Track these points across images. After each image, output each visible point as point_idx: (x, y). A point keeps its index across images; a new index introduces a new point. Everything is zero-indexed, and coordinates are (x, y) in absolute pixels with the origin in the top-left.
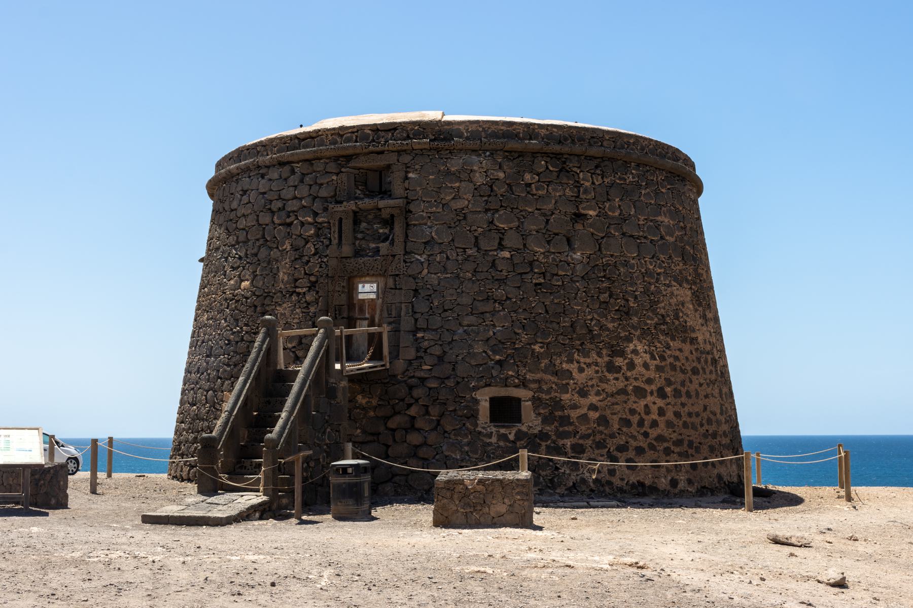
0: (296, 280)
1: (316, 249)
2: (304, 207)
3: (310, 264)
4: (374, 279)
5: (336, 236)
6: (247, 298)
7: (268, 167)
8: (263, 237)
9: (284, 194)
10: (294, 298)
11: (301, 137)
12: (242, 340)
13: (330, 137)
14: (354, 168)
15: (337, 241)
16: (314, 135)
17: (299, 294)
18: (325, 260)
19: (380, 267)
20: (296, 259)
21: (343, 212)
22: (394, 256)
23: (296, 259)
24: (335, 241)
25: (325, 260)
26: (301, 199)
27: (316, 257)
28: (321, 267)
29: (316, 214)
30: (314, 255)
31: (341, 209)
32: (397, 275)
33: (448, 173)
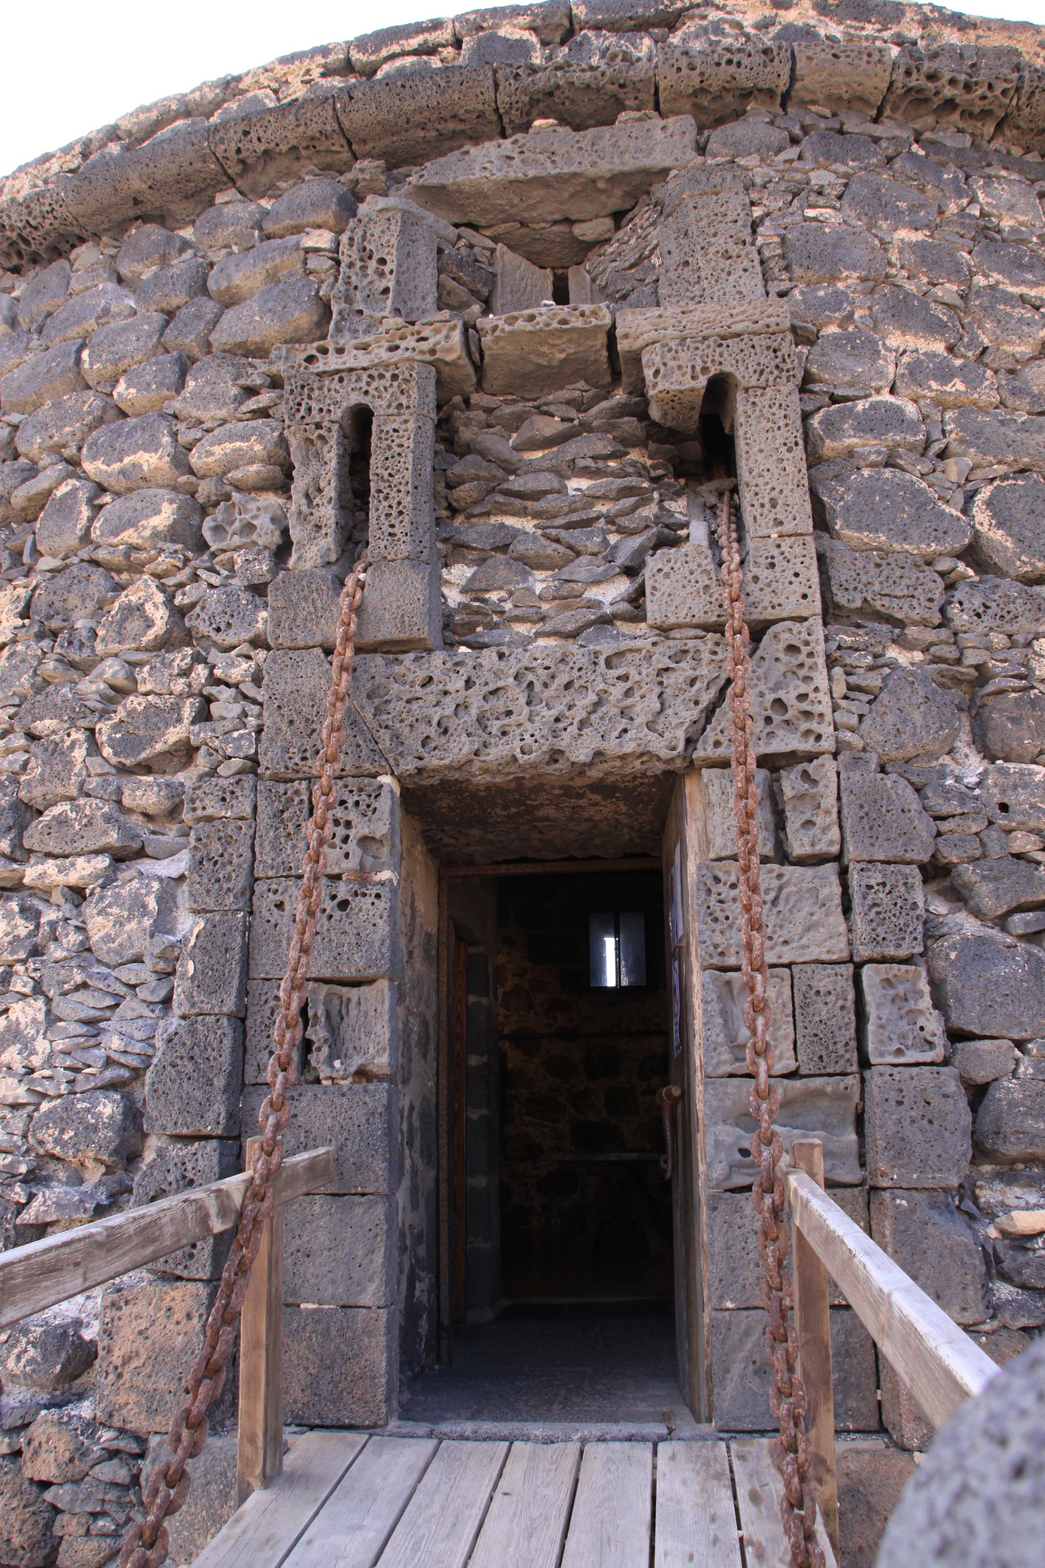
1: (179, 613)
3: (134, 702)
5: (328, 513)
14: (435, 196)
15: (327, 543)
19: (645, 706)
21: (373, 373)
22: (758, 631)
24: (313, 551)
25: (240, 670)
27: (180, 658)
28: (204, 715)
30: (164, 644)
31: (363, 360)
32: (792, 758)
33: (985, 233)
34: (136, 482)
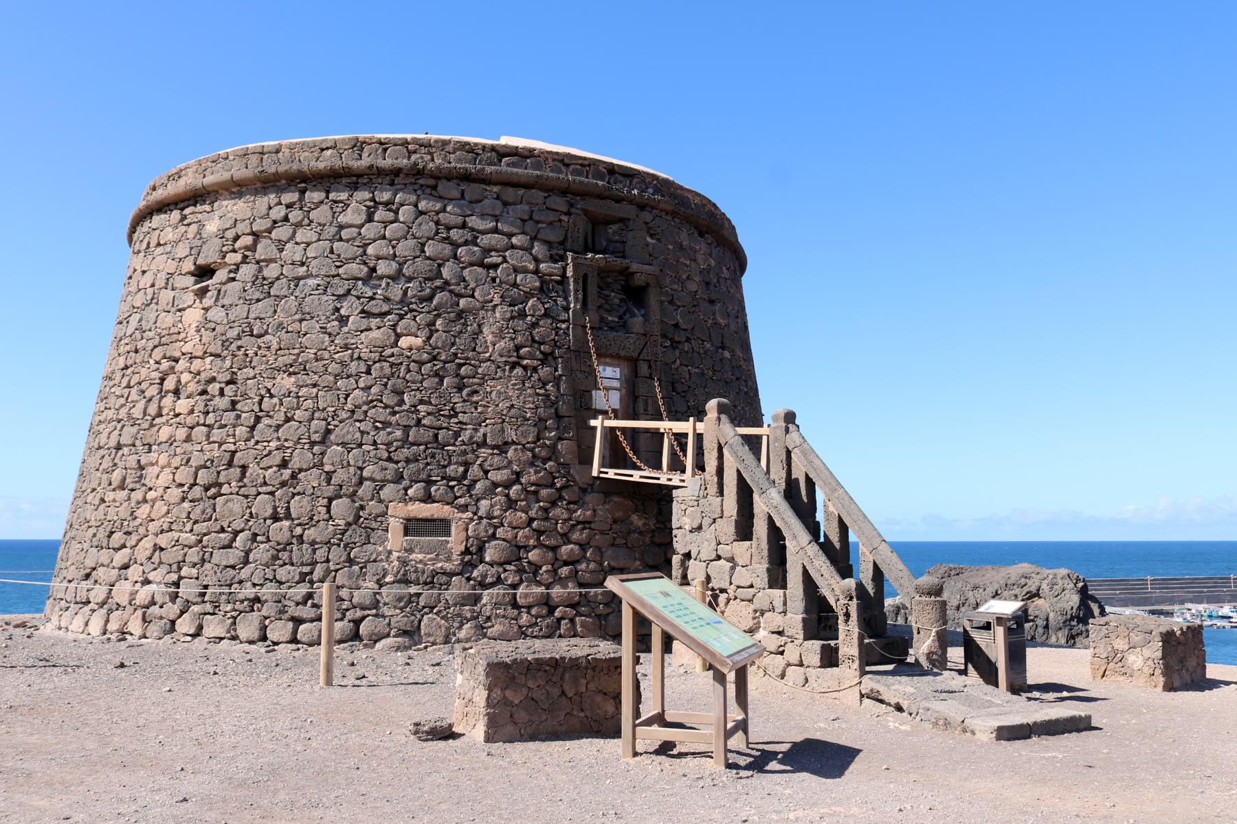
0: (518, 348)
2: (513, 247)
4: (615, 362)
6: (421, 363)
7: (437, 178)
8: (439, 275)
9: (474, 222)
10: (518, 371)
11: (501, 151)
12: (419, 423)
13: (551, 163)
16: (526, 153)
17: (525, 368)
18: (564, 326)
20: (512, 318)
23: (512, 318)
26: (510, 236)
29: (537, 260)
34: (525, 271)
